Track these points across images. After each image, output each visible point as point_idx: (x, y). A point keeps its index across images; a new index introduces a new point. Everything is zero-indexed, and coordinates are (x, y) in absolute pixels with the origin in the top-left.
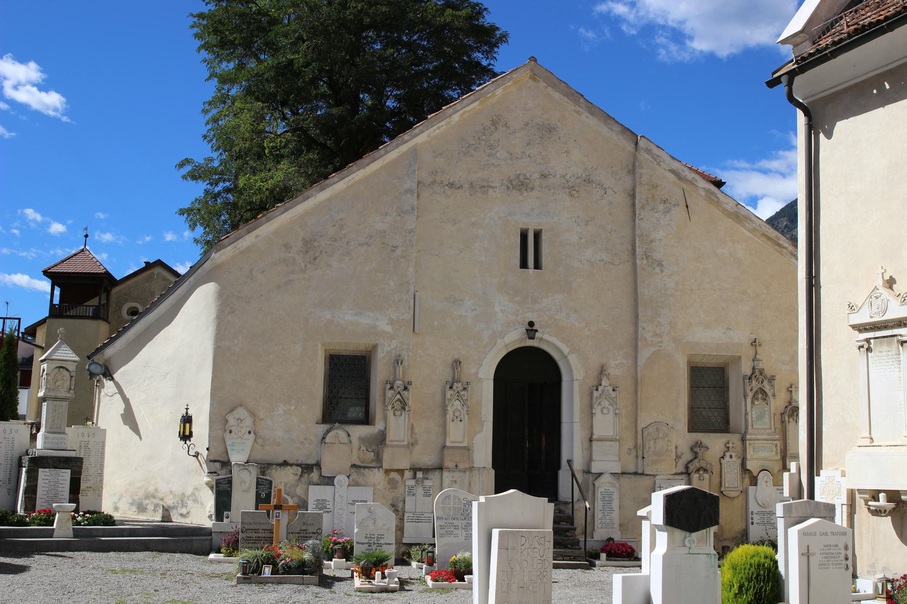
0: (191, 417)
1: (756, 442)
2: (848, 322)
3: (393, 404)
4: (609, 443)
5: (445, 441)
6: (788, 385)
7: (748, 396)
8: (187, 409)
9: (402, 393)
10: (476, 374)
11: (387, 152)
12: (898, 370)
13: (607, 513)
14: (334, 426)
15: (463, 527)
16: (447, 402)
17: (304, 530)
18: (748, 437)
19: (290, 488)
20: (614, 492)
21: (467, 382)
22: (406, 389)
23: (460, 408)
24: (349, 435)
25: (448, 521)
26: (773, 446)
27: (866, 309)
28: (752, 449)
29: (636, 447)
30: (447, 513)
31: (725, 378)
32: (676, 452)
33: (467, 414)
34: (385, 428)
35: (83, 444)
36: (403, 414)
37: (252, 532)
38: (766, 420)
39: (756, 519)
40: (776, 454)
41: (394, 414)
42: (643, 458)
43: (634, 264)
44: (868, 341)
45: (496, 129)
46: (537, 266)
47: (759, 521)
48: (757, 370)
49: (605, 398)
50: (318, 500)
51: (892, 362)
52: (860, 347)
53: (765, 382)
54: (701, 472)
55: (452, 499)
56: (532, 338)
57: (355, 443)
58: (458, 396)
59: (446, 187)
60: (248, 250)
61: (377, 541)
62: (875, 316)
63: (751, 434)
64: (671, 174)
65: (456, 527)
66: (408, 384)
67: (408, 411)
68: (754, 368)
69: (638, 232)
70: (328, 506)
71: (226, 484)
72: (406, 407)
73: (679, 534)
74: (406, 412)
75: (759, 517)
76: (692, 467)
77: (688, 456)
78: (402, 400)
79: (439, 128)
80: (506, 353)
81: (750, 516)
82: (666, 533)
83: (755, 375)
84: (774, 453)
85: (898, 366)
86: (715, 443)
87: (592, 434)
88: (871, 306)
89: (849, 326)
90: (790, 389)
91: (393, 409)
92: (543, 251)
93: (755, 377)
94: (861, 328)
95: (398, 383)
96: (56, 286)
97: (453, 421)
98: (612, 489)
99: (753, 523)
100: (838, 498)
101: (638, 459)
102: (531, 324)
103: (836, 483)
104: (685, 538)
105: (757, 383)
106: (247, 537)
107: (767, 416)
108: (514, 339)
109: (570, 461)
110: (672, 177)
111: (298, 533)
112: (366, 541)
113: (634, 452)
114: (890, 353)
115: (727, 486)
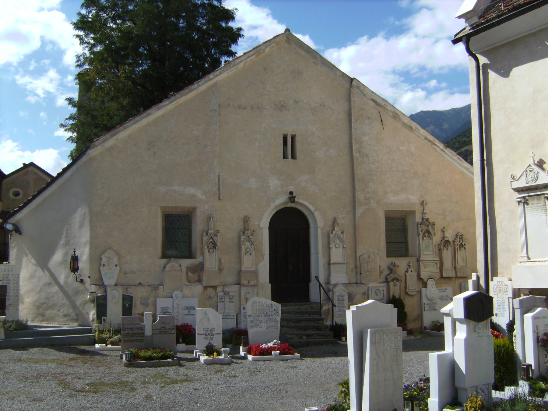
0: (78, 256)
1: (426, 262)
2: (511, 187)
3: (208, 245)
4: (340, 265)
5: (241, 267)
6: (442, 228)
7: (420, 234)
8: (75, 252)
9: (214, 238)
10: (259, 225)
11: (199, 86)
12: (545, 215)
13: (341, 308)
14: (171, 260)
15: (265, 320)
16: (242, 243)
17: (163, 327)
18: (421, 259)
19: (144, 300)
20: (345, 295)
21: (254, 230)
22: (216, 235)
23: (249, 246)
24: (180, 266)
25: (255, 318)
26: (435, 264)
27: (523, 178)
28: (423, 267)
29: (356, 267)
30: (255, 313)
31: (406, 224)
32: (380, 270)
33: (254, 250)
34: (204, 260)
35: (5, 276)
36: (214, 251)
37: (129, 330)
38: (431, 249)
39: (427, 307)
40: (437, 268)
41: (209, 251)
42: (361, 273)
43: (352, 157)
44: (524, 197)
45: (266, 72)
46: (293, 157)
47: (428, 309)
48: (425, 219)
49: (337, 238)
50: (163, 308)
51: (541, 210)
52: (519, 202)
53: (430, 226)
54: (395, 281)
55: (257, 303)
56: (293, 202)
57: (184, 270)
58: (248, 239)
59: (236, 108)
60: (112, 148)
61: (211, 332)
62: (529, 182)
63: (423, 258)
64: (372, 102)
65: (261, 321)
66: (217, 232)
67: (218, 249)
68: (423, 219)
69: (354, 137)
70: (169, 311)
71: (103, 299)
72: (216, 247)
73: (472, 323)
74: (216, 249)
75: (428, 307)
76: (390, 278)
77: (387, 272)
78: (214, 242)
79: (231, 71)
80: (276, 211)
81: (423, 306)
82: (466, 325)
83: (423, 222)
84: (436, 268)
85: (545, 213)
86: (402, 263)
87: (330, 260)
88: (527, 176)
89: (512, 189)
90: (443, 230)
91: (208, 248)
92: (297, 148)
93: (424, 223)
94: (519, 190)
95: (211, 231)
96: (489, 71)
97: (245, 254)
98: (344, 293)
99: (425, 310)
100: (505, 294)
101: (357, 274)
102: (291, 193)
103: (504, 285)
104: (475, 326)
105: (425, 227)
106: (126, 333)
107: (431, 246)
108: (280, 201)
109: (317, 277)
110: (372, 104)
111: (159, 329)
112: (204, 332)
113: (355, 270)
114: (539, 205)
115: (409, 288)
